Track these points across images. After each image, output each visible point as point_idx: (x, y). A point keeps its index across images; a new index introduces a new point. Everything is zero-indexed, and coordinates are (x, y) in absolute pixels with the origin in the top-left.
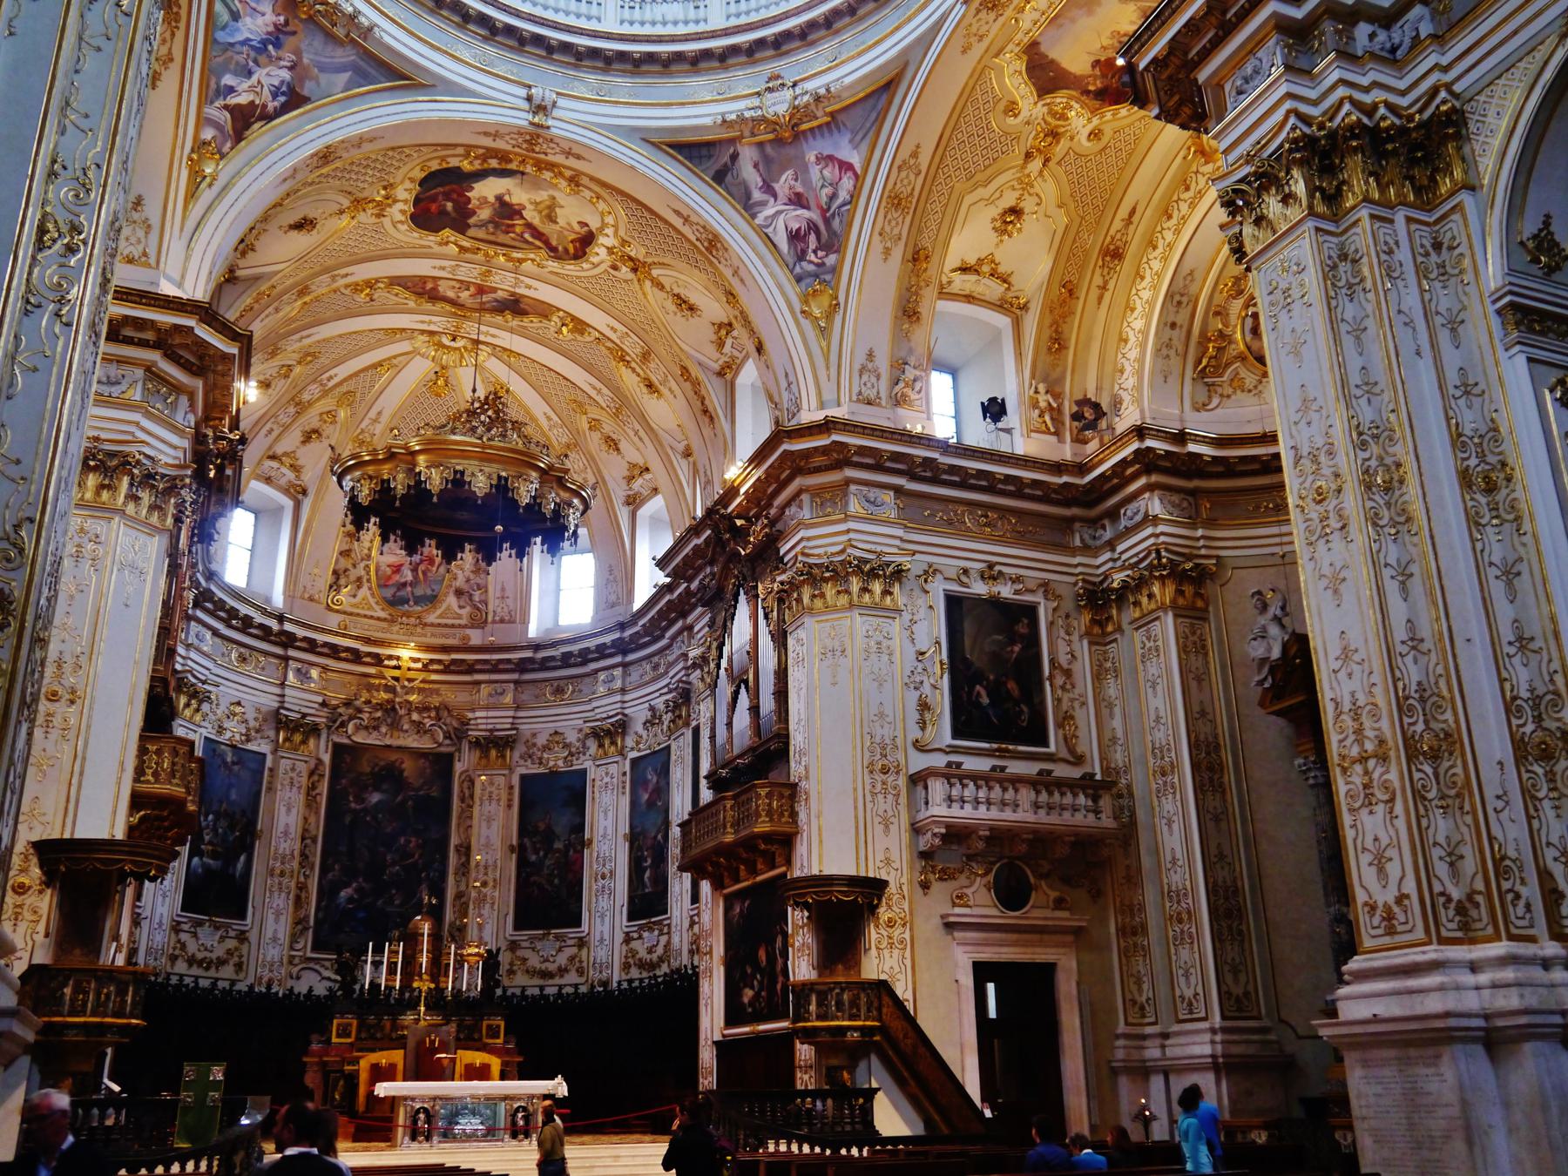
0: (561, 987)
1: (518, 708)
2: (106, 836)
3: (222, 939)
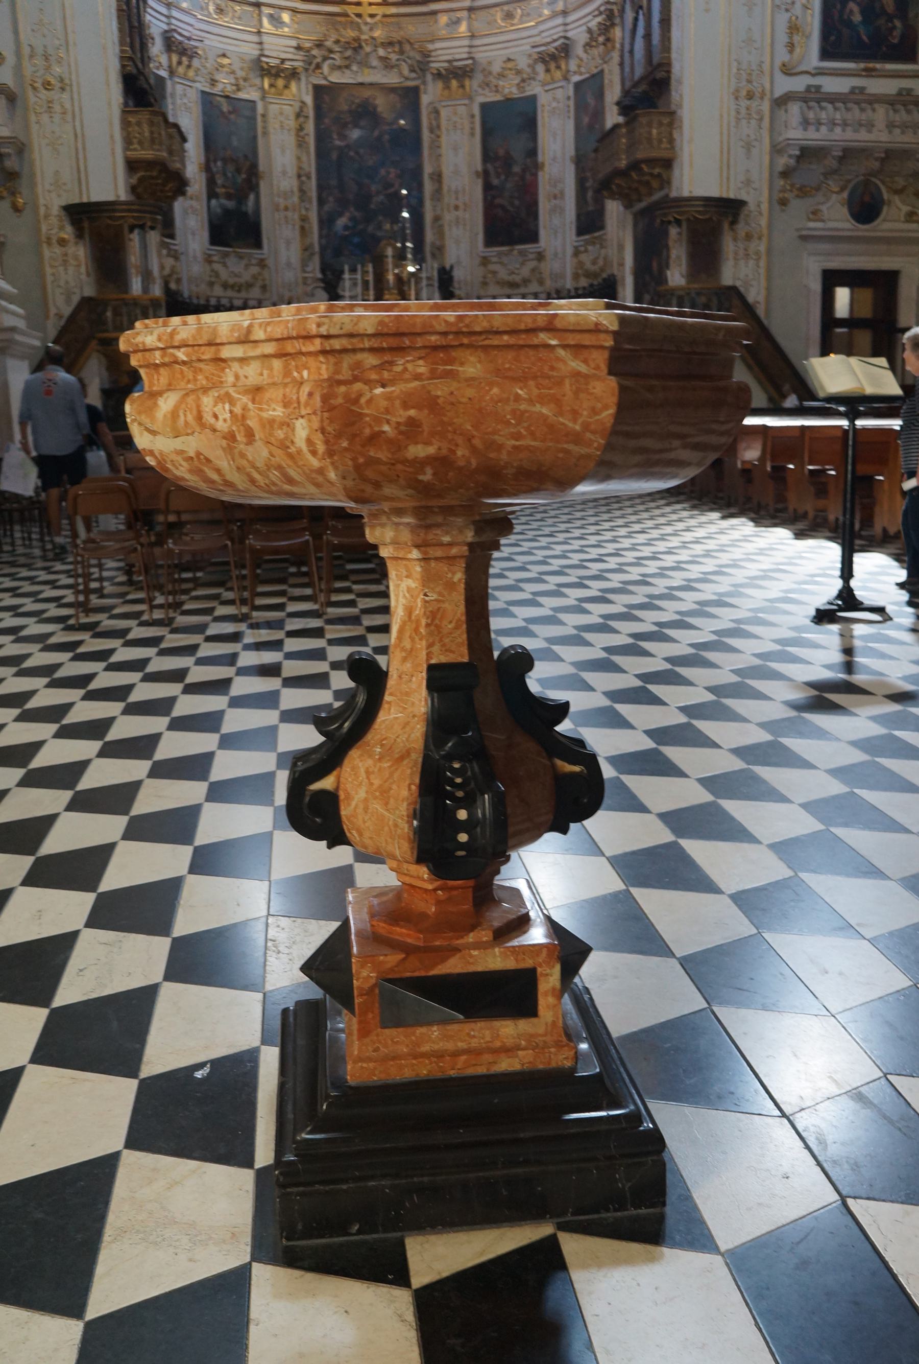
1: (473, 37)
2: (111, 198)
3: (247, 266)
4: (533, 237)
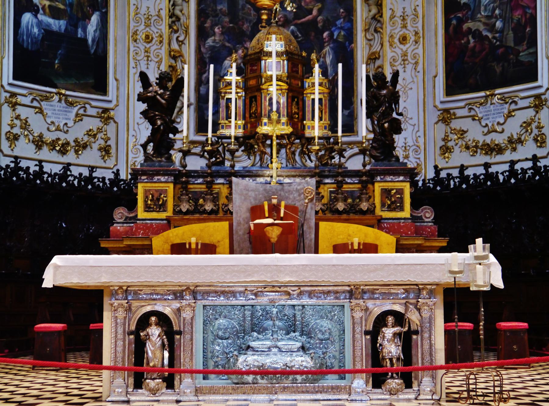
0: (513, 163)
3: (79, 118)
4: (529, 73)
